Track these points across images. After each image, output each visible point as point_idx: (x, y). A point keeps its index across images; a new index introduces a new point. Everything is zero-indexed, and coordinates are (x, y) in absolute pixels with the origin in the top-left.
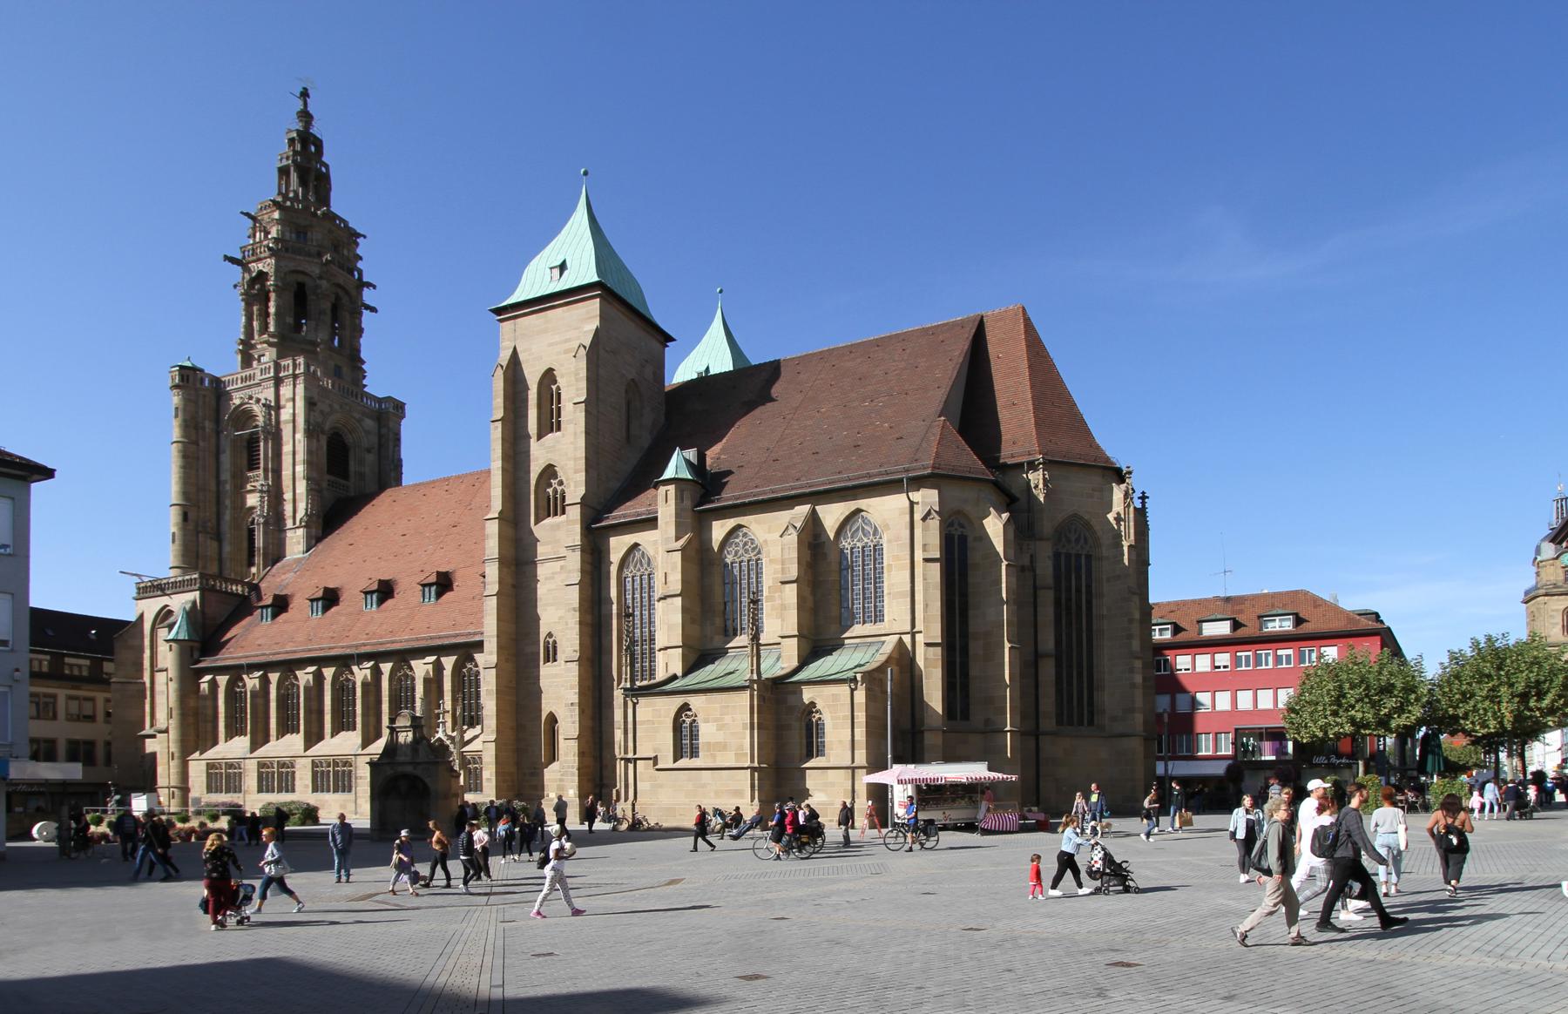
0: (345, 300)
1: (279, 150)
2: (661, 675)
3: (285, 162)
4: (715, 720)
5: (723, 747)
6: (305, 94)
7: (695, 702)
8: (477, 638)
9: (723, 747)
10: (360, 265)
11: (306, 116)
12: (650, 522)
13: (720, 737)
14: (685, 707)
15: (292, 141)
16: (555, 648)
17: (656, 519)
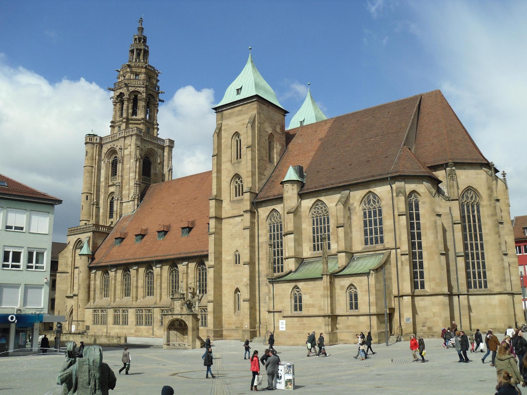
0: (152, 100)
1: (130, 43)
2: (286, 270)
3: (132, 48)
4: (309, 293)
5: (313, 306)
6: (141, 21)
7: (300, 285)
8: (205, 253)
9: (313, 306)
10: (158, 84)
11: (141, 29)
12: (280, 199)
13: (311, 302)
14: (296, 287)
15: (136, 39)
16: (239, 257)
17: (282, 198)
